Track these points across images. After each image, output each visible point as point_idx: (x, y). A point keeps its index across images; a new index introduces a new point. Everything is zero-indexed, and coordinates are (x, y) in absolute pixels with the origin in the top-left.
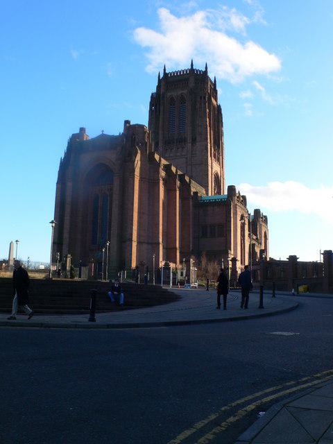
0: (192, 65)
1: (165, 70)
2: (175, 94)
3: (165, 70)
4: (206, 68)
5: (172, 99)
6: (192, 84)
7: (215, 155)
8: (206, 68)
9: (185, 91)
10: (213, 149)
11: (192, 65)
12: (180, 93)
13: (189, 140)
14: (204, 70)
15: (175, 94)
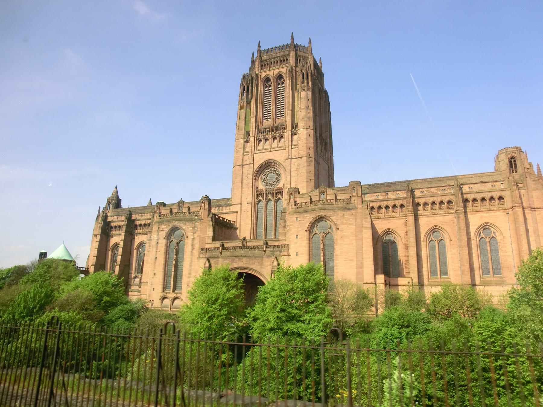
0: (292, 38)
1: (259, 46)
2: (272, 73)
3: (259, 46)
4: (310, 43)
5: (267, 79)
6: (292, 61)
7: (322, 146)
8: (310, 43)
9: (283, 70)
10: (319, 141)
11: (292, 38)
12: (276, 72)
13: (289, 127)
14: (307, 45)
15: (272, 73)
